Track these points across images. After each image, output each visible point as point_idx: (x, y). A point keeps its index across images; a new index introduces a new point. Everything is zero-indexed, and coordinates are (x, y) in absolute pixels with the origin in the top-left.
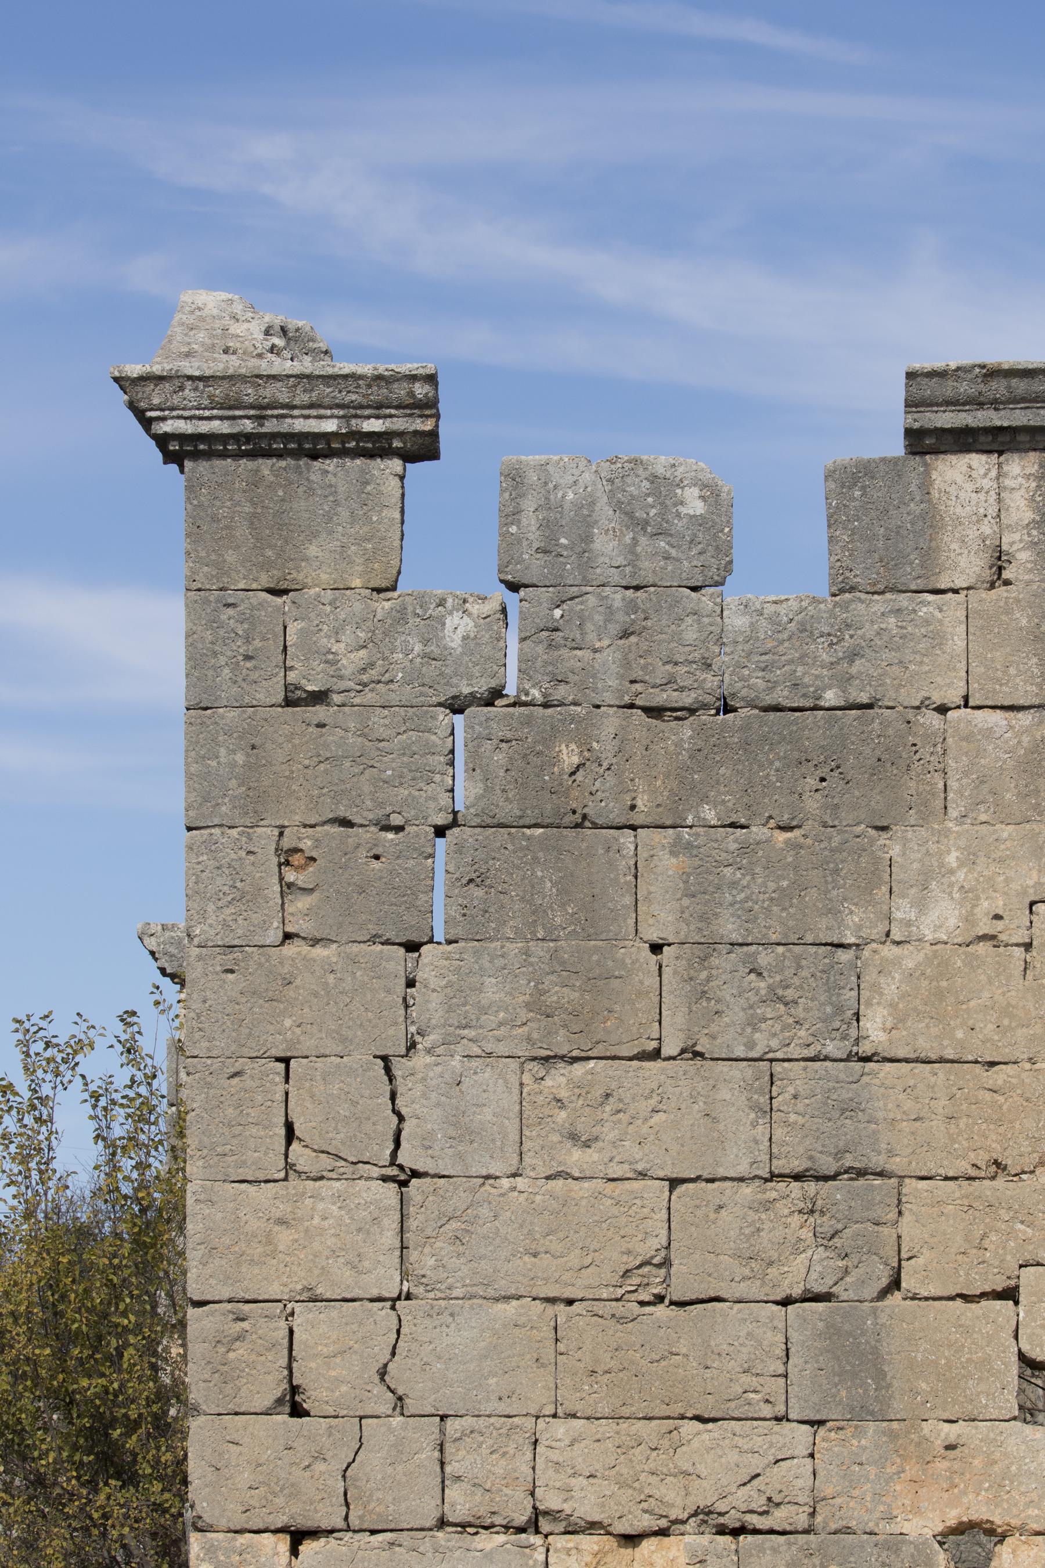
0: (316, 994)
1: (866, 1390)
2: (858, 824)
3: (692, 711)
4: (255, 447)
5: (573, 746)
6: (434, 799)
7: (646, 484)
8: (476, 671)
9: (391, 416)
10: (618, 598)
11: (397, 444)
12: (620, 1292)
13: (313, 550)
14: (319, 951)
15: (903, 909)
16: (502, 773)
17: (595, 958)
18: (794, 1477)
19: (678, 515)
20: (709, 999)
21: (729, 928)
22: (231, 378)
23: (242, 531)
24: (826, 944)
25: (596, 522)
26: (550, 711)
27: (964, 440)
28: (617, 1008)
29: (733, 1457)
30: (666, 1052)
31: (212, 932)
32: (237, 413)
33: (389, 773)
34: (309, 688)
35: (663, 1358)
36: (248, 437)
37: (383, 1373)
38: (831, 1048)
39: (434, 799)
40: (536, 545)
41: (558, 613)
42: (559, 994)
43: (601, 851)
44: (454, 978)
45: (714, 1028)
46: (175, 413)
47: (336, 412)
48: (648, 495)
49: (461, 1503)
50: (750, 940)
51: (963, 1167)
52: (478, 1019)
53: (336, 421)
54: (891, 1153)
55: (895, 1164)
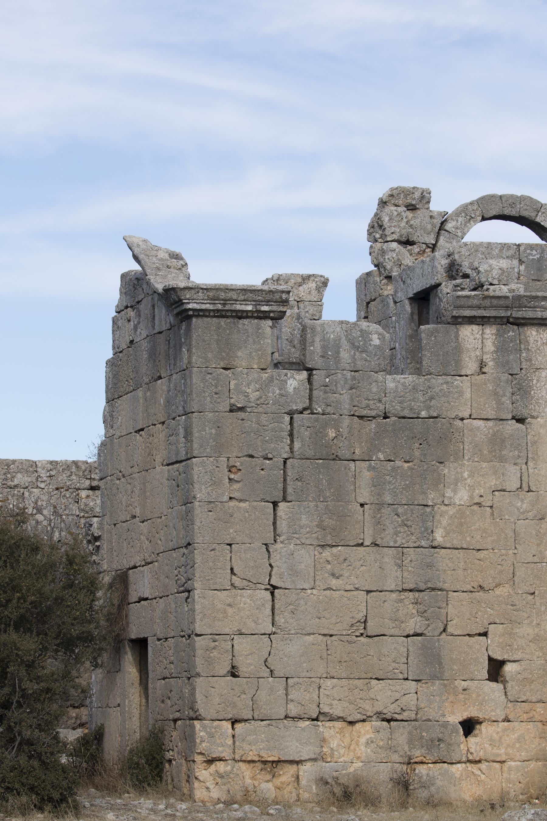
0: (241, 521)
1: (435, 669)
2: (433, 461)
3: (374, 417)
4: (220, 314)
5: (333, 430)
6: (284, 448)
7: (359, 333)
8: (298, 401)
9: (272, 305)
10: (349, 375)
11: (272, 315)
12: (350, 632)
13: (239, 354)
14: (242, 505)
15: (449, 493)
17: (341, 509)
18: (410, 701)
19: (370, 345)
20: (381, 525)
21: (388, 498)
22: (217, 289)
23: (214, 346)
24: (422, 505)
25: (341, 346)
26: (324, 416)
27: (471, 320)
28: (349, 527)
29: (389, 693)
30: (367, 543)
31: (204, 496)
32: (217, 302)
33: (267, 438)
34: (238, 406)
35: (365, 657)
36: (218, 311)
37: (266, 661)
38: (423, 543)
39: (284, 448)
40: (320, 354)
41: (327, 380)
42: (328, 522)
43: (343, 469)
44: (291, 515)
45: (383, 535)
46: (194, 301)
47: (252, 303)
48: (359, 337)
49: (293, 709)
50: (395, 503)
51: (469, 587)
52: (299, 531)
53: (252, 306)
54: (444, 582)
55: (446, 586)
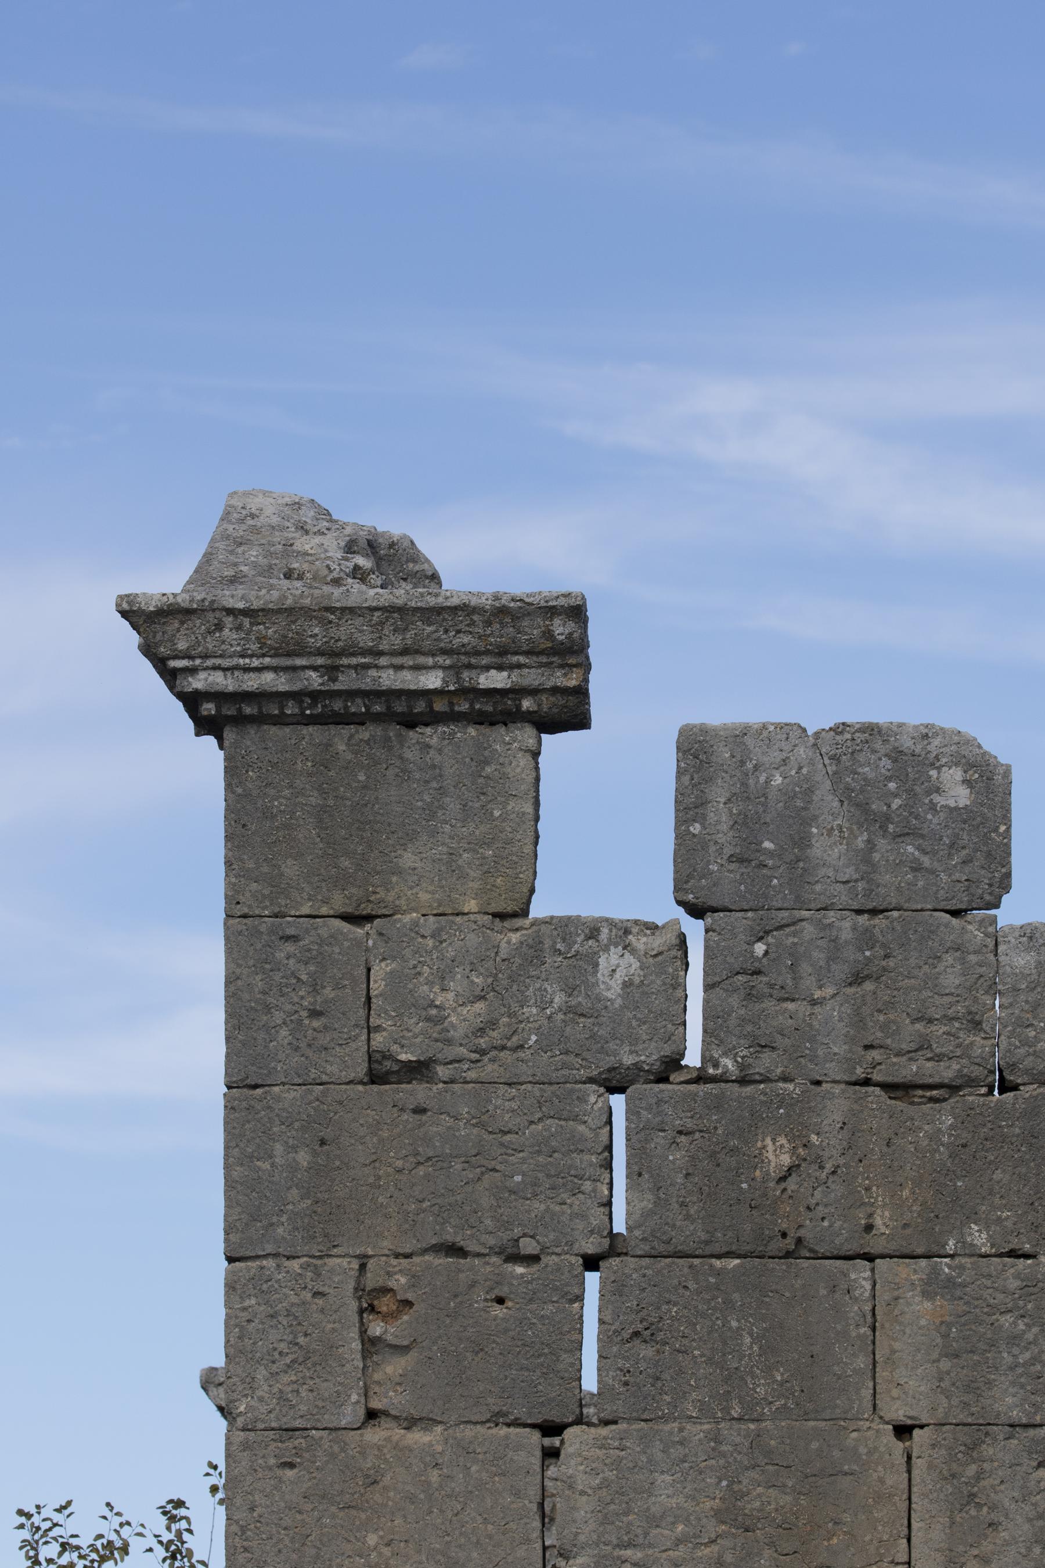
0: (412, 1499)
3: (953, 1088)
4: (323, 710)
6: (583, 1216)
7: (886, 763)
8: (643, 1032)
9: (519, 666)
10: (846, 927)
11: (526, 704)
13: (408, 859)
14: (418, 1437)
16: (680, 1179)
17: (815, 1445)
19: (933, 807)
20: (979, 1506)
21: (1008, 1402)
22: (290, 611)
25: (815, 818)
26: (749, 1090)
28: (847, 1518)
31: (264, 1409)
32: (299, 662)
33: (518, 1178)
34: (403, 1057)
36: (315, 696)
39: (583, 1216)
40: (728, 851)
41: (760, 948)
43: (823, 1292)
44: (611, 1475)
45: (987, 1547)
46: (209, 663)
47: (440, 660)
48: (889, 779)
52: (646, 1534)
53: (440, 674)
